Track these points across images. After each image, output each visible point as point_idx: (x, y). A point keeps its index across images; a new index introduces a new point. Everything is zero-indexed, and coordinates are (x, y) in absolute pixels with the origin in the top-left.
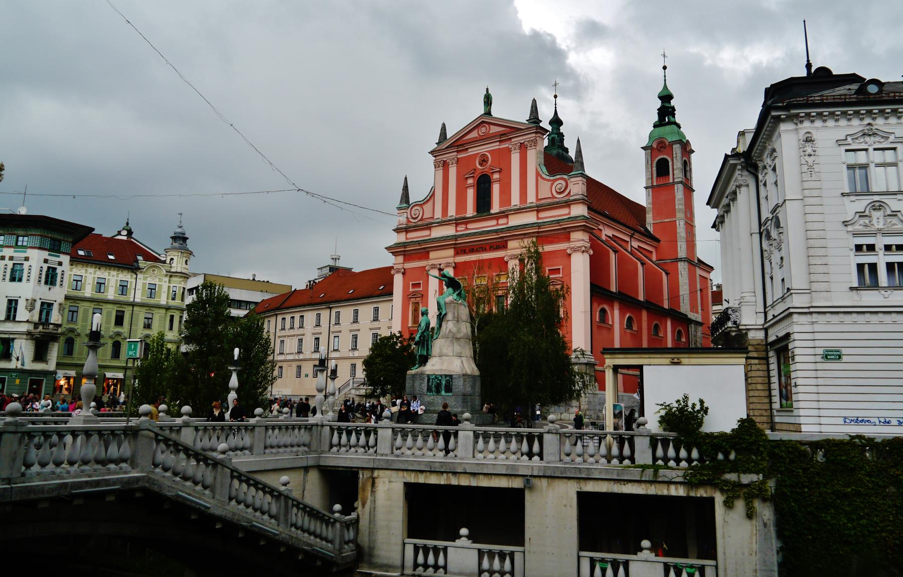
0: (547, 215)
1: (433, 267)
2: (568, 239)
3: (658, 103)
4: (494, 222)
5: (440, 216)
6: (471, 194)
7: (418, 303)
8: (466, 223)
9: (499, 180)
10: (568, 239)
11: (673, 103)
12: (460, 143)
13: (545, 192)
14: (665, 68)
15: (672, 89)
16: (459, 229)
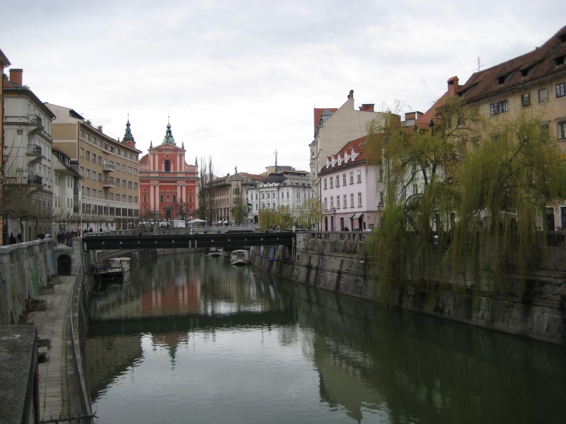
0: (189, 176)
1: (152, 185)
2: (195, 183)
3: (167, 129)
4: (172, 175)
5: (152, 170)
6: (163, 165)
7: (146, 196)
8: (162, 174)
9: (173, 163)
10: (195, 183)
11: (171, 129)
12: (158, 149)
13: (187, 169)
14: (169, 117)
15: (171, 124)
16: (160, 175)
